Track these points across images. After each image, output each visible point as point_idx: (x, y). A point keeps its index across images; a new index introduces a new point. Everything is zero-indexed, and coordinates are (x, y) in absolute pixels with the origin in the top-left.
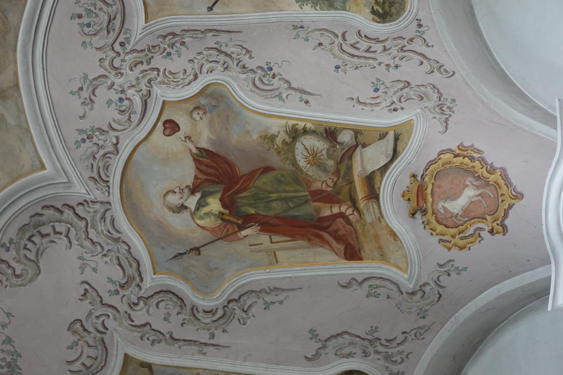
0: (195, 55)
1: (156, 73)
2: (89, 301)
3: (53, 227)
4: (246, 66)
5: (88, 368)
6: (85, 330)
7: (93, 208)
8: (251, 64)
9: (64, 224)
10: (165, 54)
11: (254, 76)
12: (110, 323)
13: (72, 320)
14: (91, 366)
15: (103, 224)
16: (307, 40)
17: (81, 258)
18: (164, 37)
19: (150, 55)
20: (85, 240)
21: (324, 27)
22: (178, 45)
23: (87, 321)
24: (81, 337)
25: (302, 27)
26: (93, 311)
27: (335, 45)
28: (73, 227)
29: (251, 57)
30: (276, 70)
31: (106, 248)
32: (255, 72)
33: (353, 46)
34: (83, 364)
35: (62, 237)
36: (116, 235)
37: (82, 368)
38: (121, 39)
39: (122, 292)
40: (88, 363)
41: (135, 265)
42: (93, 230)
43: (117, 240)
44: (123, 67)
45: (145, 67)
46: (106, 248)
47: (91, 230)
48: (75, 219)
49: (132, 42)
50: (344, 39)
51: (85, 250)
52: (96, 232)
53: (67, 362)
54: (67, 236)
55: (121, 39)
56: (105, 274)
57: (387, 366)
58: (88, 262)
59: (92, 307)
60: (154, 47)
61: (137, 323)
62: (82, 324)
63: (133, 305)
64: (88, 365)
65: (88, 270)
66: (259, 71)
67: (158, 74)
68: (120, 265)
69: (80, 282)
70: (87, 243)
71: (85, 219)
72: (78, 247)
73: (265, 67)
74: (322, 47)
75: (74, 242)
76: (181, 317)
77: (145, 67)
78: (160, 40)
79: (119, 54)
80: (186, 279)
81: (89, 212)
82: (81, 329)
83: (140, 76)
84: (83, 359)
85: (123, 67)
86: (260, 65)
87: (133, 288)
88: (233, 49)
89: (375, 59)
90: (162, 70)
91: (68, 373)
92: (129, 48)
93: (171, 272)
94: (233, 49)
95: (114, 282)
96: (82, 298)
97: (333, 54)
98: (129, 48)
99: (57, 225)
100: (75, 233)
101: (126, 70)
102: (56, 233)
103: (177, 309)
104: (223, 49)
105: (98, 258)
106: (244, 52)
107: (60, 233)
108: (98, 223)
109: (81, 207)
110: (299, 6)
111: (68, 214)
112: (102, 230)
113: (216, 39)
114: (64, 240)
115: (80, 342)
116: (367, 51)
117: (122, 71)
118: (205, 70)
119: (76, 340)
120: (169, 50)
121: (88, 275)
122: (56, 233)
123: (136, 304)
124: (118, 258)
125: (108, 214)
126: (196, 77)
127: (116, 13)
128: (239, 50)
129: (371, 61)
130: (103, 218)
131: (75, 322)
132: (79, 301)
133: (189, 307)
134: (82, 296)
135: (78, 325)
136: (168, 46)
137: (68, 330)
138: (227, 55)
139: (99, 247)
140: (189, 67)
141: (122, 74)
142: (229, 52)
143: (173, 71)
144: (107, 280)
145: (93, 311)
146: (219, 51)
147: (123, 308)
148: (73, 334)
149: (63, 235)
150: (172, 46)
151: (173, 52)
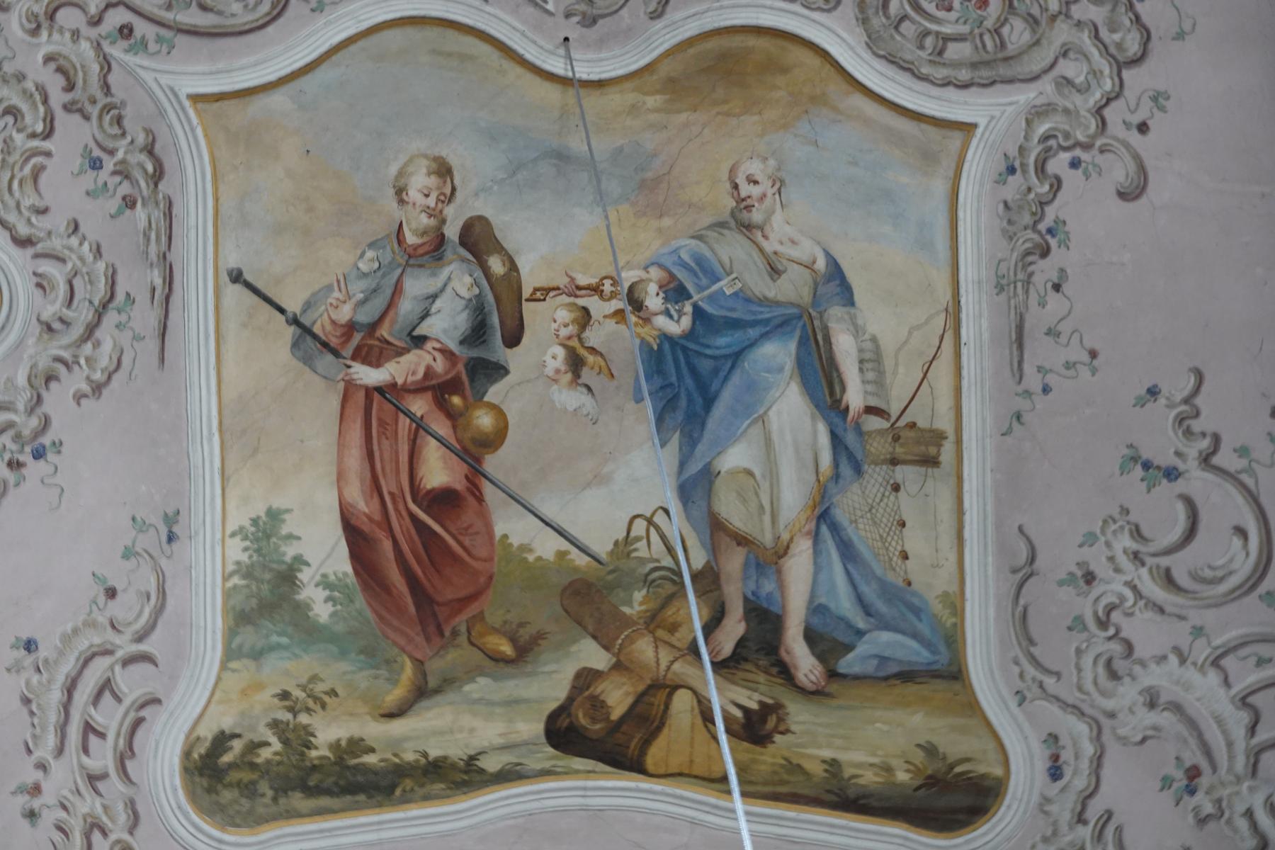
0: (92, 237)
1: (39, 128)
4: (53, 385)
8: (58, 400)
10: (97, 153)
11: (21, 406)
16: (128, 554)
18: (150, 150)
19: (94, 111)
21: (171, 602)
22: (126, 188)
25: (171, 538)
27: (110, 635)
29: (79, 397)
30: (35, 469)
32: (31, 411)
33: (106, 686)
38: (142, 28)
44: (56, 36)
45: (58, 97)
49: (130, 59)
50: (127, 662)
55: (142, 28)
60: (119, 120)
66: (34, 422)
67: (33, 136)
73: (46, 440)
74: (102, 599)
77: (58, 97)
78: (141, 139)
79: (96, 21)
83: (30, 85)
85: (56, 36)
86: (55, 423)
88: (107, 346)
89: (60, 751)
90: (47, 145)
92: (116, 51)
94: (107, 346)
97: (76, 631)
98: (116, 51)
101: (46, 43)
104: (111, 318)
106: (98, 376)
110: (242, 528)
113: (142, 297)
116: (89, 728)
117: (44, 34)
118: (46, 267)
120: (109, 164)
126: (23, 242)
127: (220, 13)
128: (104, 361)
129: (51, 740)
136: (123, 162)
138: (91, 330)
140: (57, 221)
141: (35, 32)
142: (98, 334)
143: (43, 179)
146: (105, 306)
150: (123, 172)
151: (104, 175)
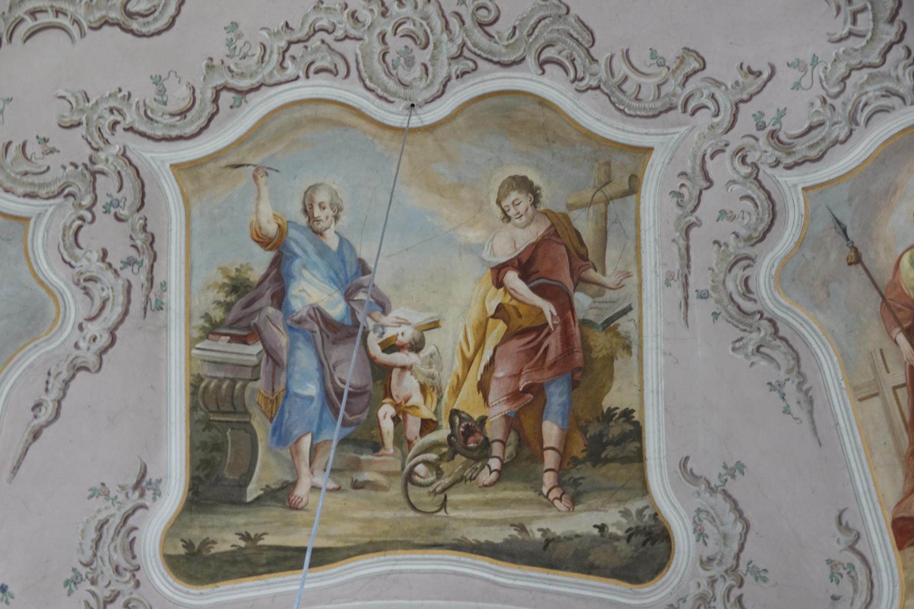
2: (741, 79)
3: (864, 9)
5: (619, 87)
6: (687, 77)
7: (904, 74)
9: (871, 26)
12: (704, 117)
13: (702, 54)
14: (623, 92)
15: (878, 93)
17: (815, 61)
20: (847, 65)
23: (705, 79)
24: (674, 72)
26: (723, 88)
28: (868, 42)
31: (837, 103)
34: (626, 78)
35: (849, 26)
36: (861, 118)
37: (618, 77)
39: (762, 135)
40: (629, 87)
41: (813, 154)
42: (866, 77)
43: (853, 120)
46: (837, 103)
47: (865, 73)
48: (882, 46)
51: (829, 66)
52: (863, 84)
53: (627, 51)
54: (850, 34)
56: (792, 104)
57: (688, 599)
58: (809, 72)
59: (729, 86)
61: (710, 165)
62: (698, 71)
63: (742, 155)
64: (624, 87)
65: (794, 75)
68: (811, 128)
69: (772, 62)
70: (842, 69)
71: (884, 63)
72: (834, 55)
75: (841, 48)
76: (731, 240)
80: (800, 244)
81: (896, 67)
82: (688, 69)
84: (634, 78)
87: (772, 154)
91: (608, 55)
93: (809, 217)
95: (778, 120)
96: (745, 67)
99: (868, 15)
100: (857, 47)
102: (855, 15)
103: (743, 232)
105: (817, 90)
107: (854, 22)
108: (879, 86)
109: (903, 53)
111: (890, 33)
112: (867, 93)
114: (843, 29)
115: (665, 70)
119: (667, 64)
121: (786, 76)
122: (855, 15)
123: (743, 161)
124: (821, 124)
125: (896, 101)
130: (889, 93)
131: (700, 60)
132: (738, 64)
133: (750, 251)
134: (749, 68)
135: (696, 65)
137: (685, 49)
139: (837, 89)
144: (781, 109)
145: (723, 88)
147: (735, 139)
148: (678, 58)
149: (852, 27)
